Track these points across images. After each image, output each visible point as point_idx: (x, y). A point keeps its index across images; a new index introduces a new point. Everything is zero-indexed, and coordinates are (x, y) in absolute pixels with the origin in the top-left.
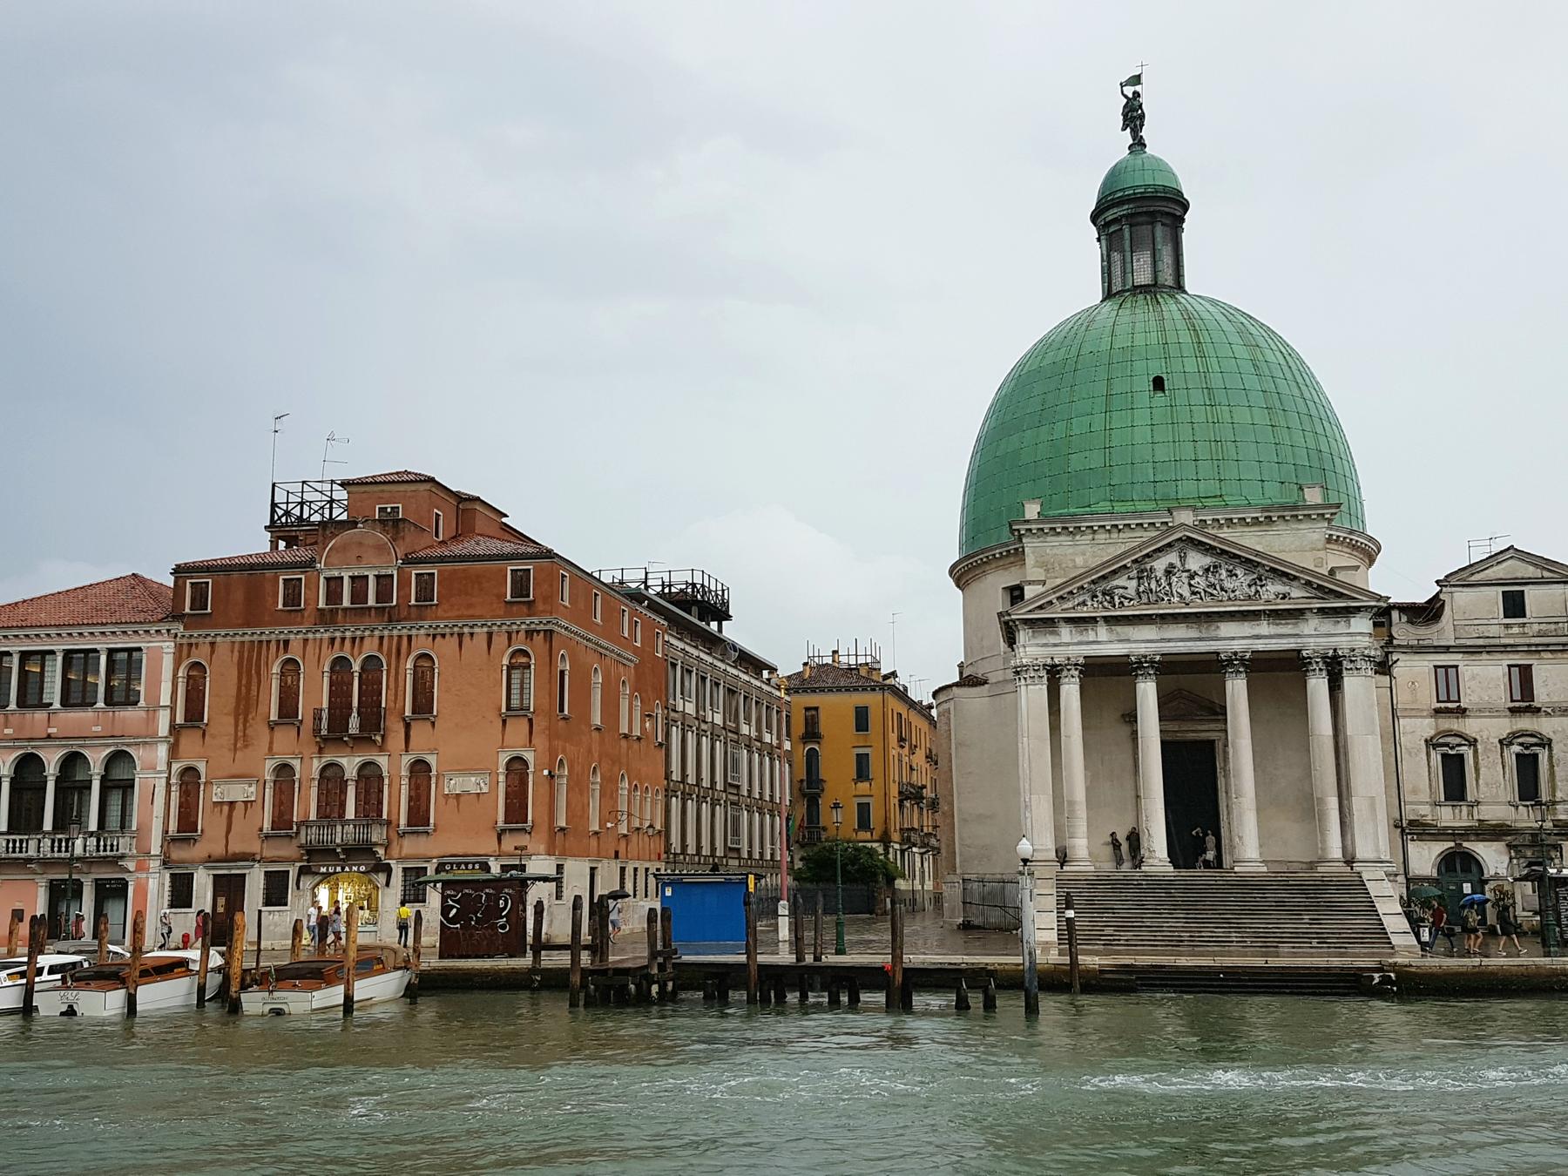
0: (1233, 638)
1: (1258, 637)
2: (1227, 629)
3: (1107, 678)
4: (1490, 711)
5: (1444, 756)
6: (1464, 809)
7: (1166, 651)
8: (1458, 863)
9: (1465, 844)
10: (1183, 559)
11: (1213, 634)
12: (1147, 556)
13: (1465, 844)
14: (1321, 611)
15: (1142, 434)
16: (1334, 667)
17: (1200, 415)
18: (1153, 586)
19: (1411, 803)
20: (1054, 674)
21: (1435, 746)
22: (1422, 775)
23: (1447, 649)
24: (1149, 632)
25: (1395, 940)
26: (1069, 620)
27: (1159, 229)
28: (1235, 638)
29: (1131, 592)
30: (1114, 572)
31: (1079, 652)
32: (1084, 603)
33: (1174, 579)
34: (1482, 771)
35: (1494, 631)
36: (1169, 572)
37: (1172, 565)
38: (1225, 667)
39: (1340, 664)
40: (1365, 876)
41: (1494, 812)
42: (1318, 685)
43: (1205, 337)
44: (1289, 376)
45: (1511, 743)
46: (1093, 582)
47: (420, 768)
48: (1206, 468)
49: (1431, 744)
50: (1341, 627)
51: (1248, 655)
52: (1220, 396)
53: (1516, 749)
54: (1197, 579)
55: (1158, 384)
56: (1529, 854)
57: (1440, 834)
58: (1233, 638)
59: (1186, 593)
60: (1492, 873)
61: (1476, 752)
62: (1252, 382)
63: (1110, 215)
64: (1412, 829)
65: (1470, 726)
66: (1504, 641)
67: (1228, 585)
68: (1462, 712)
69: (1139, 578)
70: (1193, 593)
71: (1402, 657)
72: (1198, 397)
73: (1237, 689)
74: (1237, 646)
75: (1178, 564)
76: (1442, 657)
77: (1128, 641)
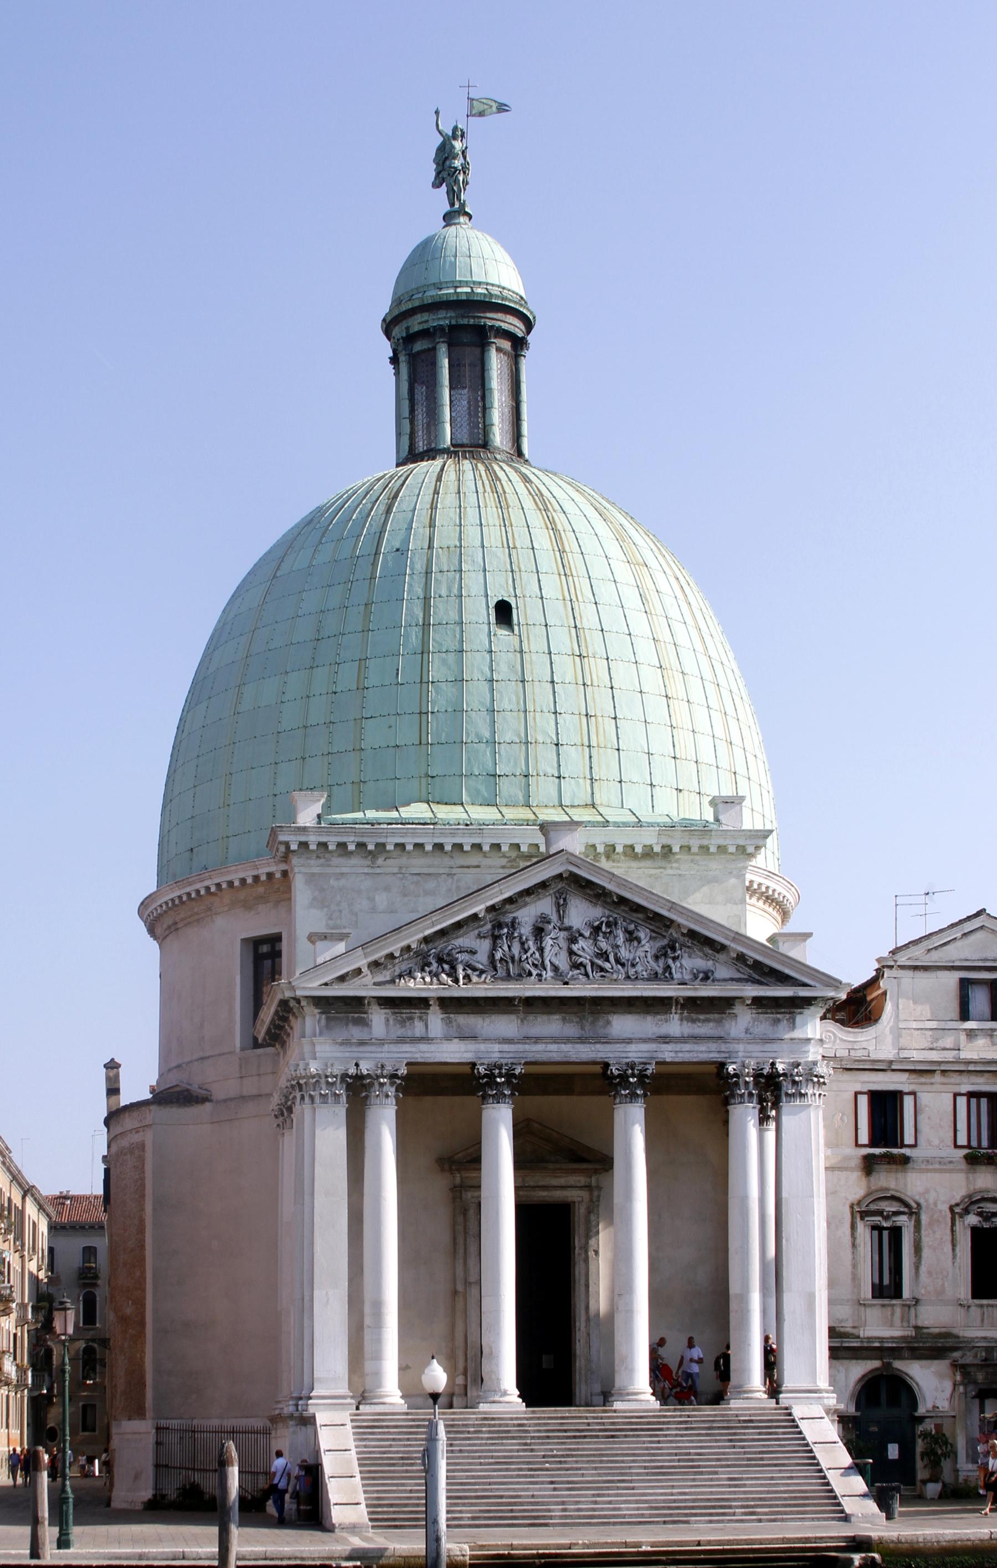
0: (629, 1041)
1: (665, 1039)
2: (622, 1024)
3: (442, 1095)
4: (943, 1165)
6: (898, 1311)
9: (898, 1364)
10: (561, 907)
11: (601, 1032)
12: (510, 900)
13: (898, 1364)
15: (475, 695)
16: (772, 1090)
17: (566, 669)
18: (516, 949)
21: (864, 1215)
23: (887, 1067)
24: (505, 1025)
25: (849, 1506)
28: (634, 1042)
29: (481, 959)
30: (458, 925)
32: (410, 974)
33: (548, 942)
34: (926, 1253)
36: (539, 932)
37: (545, 919)
38: (615, 1087)
39: (778, 1087)
40: (797, 1412)
45: (966, 1211)
46: (426, 940)
48: (574, 761)
49: (861, 1212)
51: (651, 1069)
53: (973, 1219)
54: (582, 943)
56: (980, 1377)
58: (629, 1041)
59: (563, 962)
60: (930, 1406)
63: (416, 324)
65: (913, 1184)
66: (965, 1055)
67: (624, 954)
68: (905, 1160)
69: (495, 938)
70: (576, 966)
72: (562, 640)
74: (635, 1053)
75: (554, 917)
76: (880, 1077)
77: (474, 1038)
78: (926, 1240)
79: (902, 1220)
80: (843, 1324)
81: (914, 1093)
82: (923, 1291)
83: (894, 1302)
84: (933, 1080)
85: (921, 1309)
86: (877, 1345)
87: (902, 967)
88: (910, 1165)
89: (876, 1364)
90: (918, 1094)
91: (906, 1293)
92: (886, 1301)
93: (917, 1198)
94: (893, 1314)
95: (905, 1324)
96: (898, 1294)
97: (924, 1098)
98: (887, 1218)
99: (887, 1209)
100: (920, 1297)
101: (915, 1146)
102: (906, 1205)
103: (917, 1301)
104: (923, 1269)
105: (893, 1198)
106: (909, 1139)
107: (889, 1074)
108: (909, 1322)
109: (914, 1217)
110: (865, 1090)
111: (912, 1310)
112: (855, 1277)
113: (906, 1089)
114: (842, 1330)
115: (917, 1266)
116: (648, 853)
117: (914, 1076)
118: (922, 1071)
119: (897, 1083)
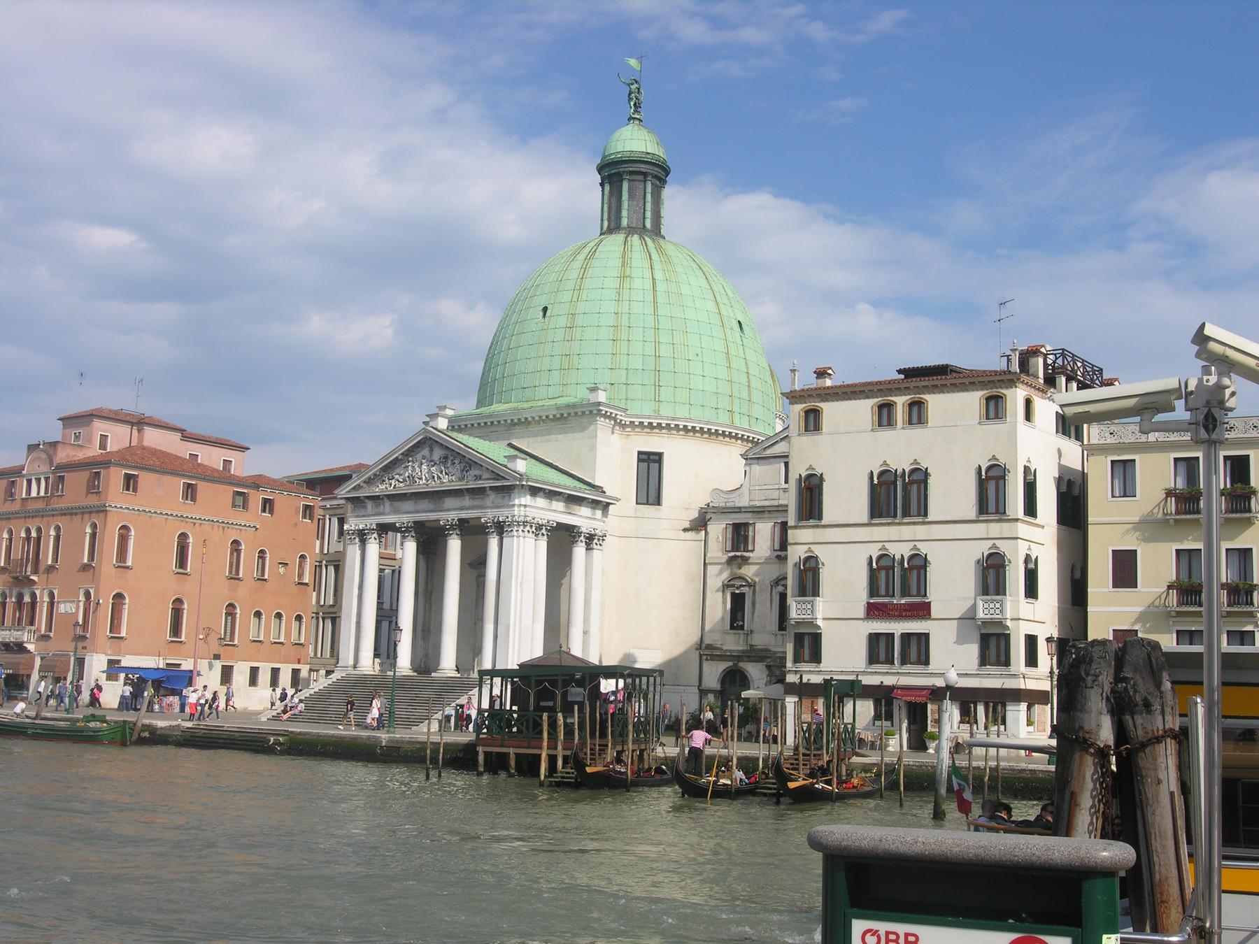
2: (449, 502)
5: (733, 594)
7: (417, 519)
8: (735, 679)
9: (741, 664)
10: (431, 451)
13: (741, 664)
14: (491, 488)
16: (501, 528)
20: (362, 536)
21: (728, 586)
23: (739, 510)
24: (408, 505)
26: (368, 497)
27: (625, 186)
31: (372, 522)
34: (757, 606)
35: (775, 494)
41: (759, 640)
42: (493, 542)
43: (589, 274)
44: (649, 297)
47: (52, 595)
49: (725, 586)
50: (506, 501)
52: (579, 321)
53: (780, 589)
55: (545, 310)
62: (612, 307)
71: (713, 516)
72: (562, 321)
73: (454, 546)
76: (739, 515)
78: (758, 599)
89: (731, 664)
97: (759, 526)
115: (753, 613)
116: (555, 419)
118: (760, 512)
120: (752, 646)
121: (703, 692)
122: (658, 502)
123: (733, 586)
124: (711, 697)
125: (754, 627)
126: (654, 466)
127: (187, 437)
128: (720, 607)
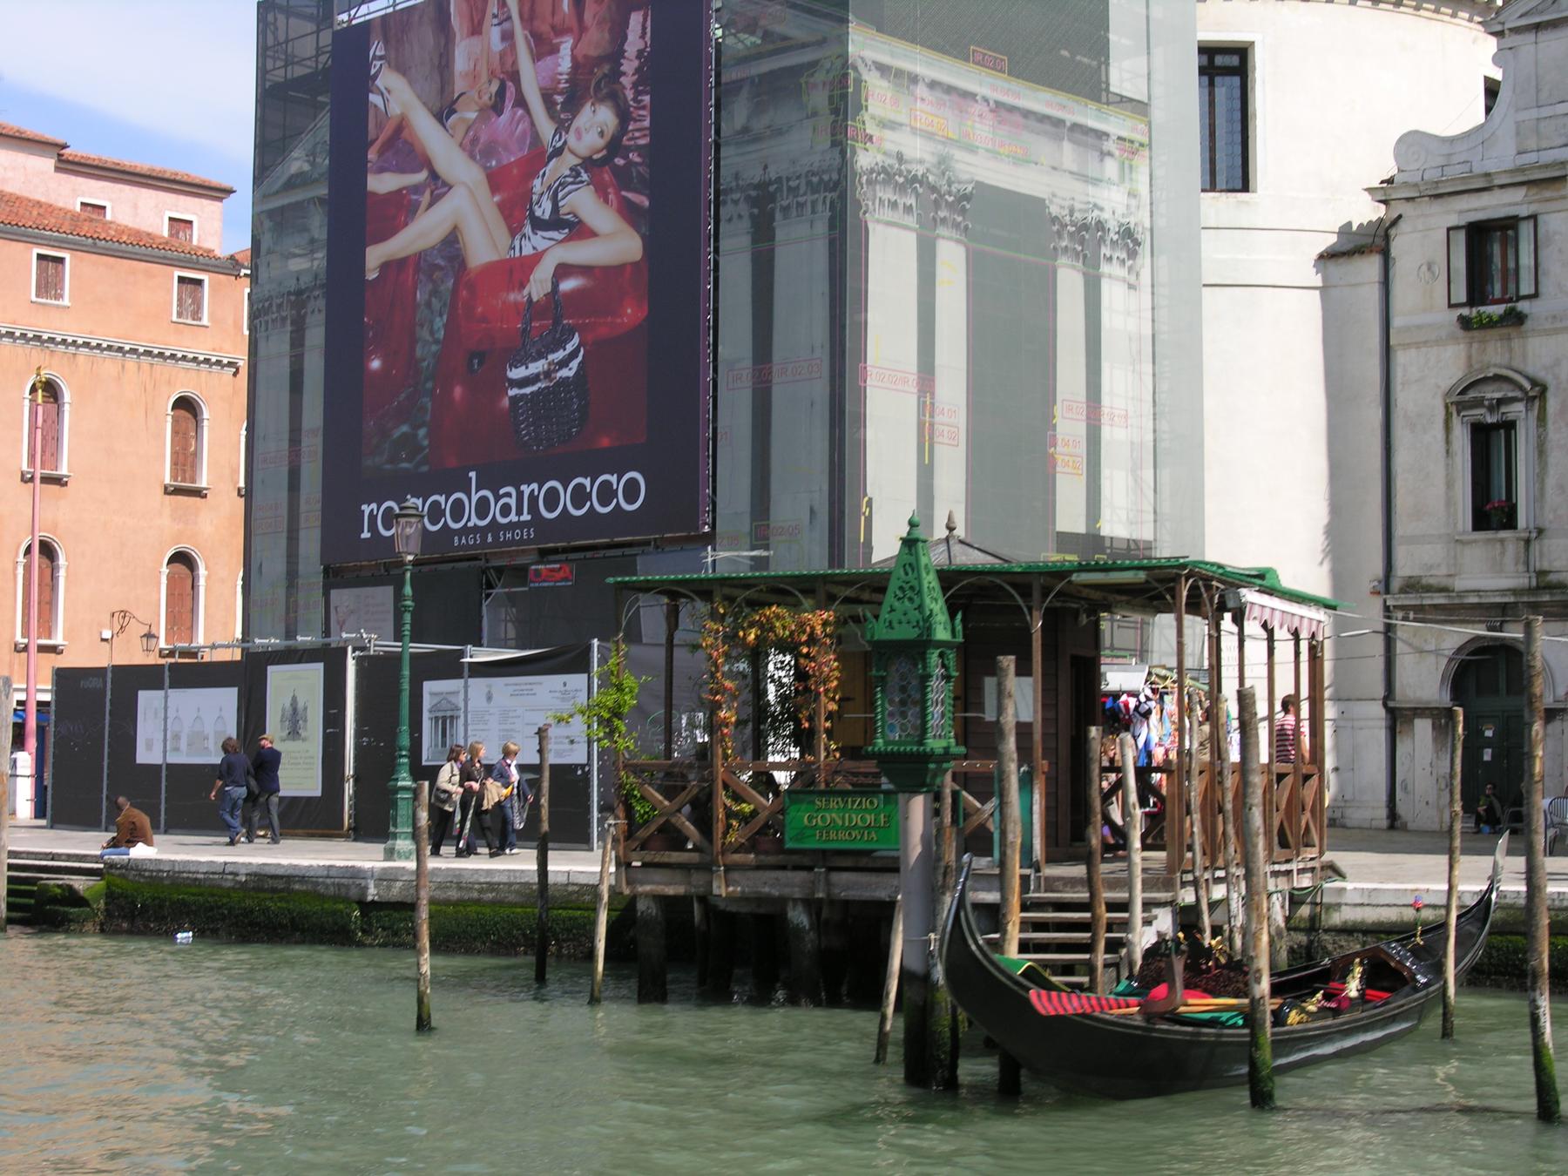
6: (1511, 549)
19: (1412, 540)
21: (1461, 406)
22: (1436, 474)
34: (1554, 457)
57: (1455, 611)
61: (1542, 419)
64: (1407, 599)
78: (1554, 434)
79: (1516, 410)
80: (1433, 572)
81: (1534, 217)
82: (1551, 516)
83: (1503, 534)
84: (1563, 192)
85: (1546, 542)
86: (1473, 600)
87: (1516, 30)
88: (1528, 324)
90: (1541, 219)
91: (1522, 521)
92: (1489, 535)
93: (1541, 375)
94: (1503, 553)
95: (1521, 568)
96: (1510, 522)
98: (1491, 409)
99: (1489, 396)
100: (1547, 525)
101: (1536, 295)
102: (1521, 388)
103: (1540, 531)
104: (1551, 481)
105: (1498, 378)
106: (1526, 288)
107: (1497, 193)
108: (1527, 564)
109: (1537, 403)
110: (1463, 223)
111: (1535, 547)
112: (1449, 502)
113: (1523, 211)
114: (1432, 581)
117: (1534, 191)
119: (1510, 205)
120: (1541, 573)
121: (1398, 718)
122: (1245, 187)
123: (1478, 403)
124: (1423, 727)
125: (1547, 519)
126: (1226, 87)
127: (69, 165)
128: (1438, 470)
